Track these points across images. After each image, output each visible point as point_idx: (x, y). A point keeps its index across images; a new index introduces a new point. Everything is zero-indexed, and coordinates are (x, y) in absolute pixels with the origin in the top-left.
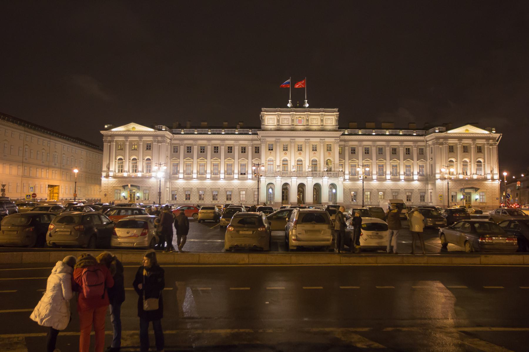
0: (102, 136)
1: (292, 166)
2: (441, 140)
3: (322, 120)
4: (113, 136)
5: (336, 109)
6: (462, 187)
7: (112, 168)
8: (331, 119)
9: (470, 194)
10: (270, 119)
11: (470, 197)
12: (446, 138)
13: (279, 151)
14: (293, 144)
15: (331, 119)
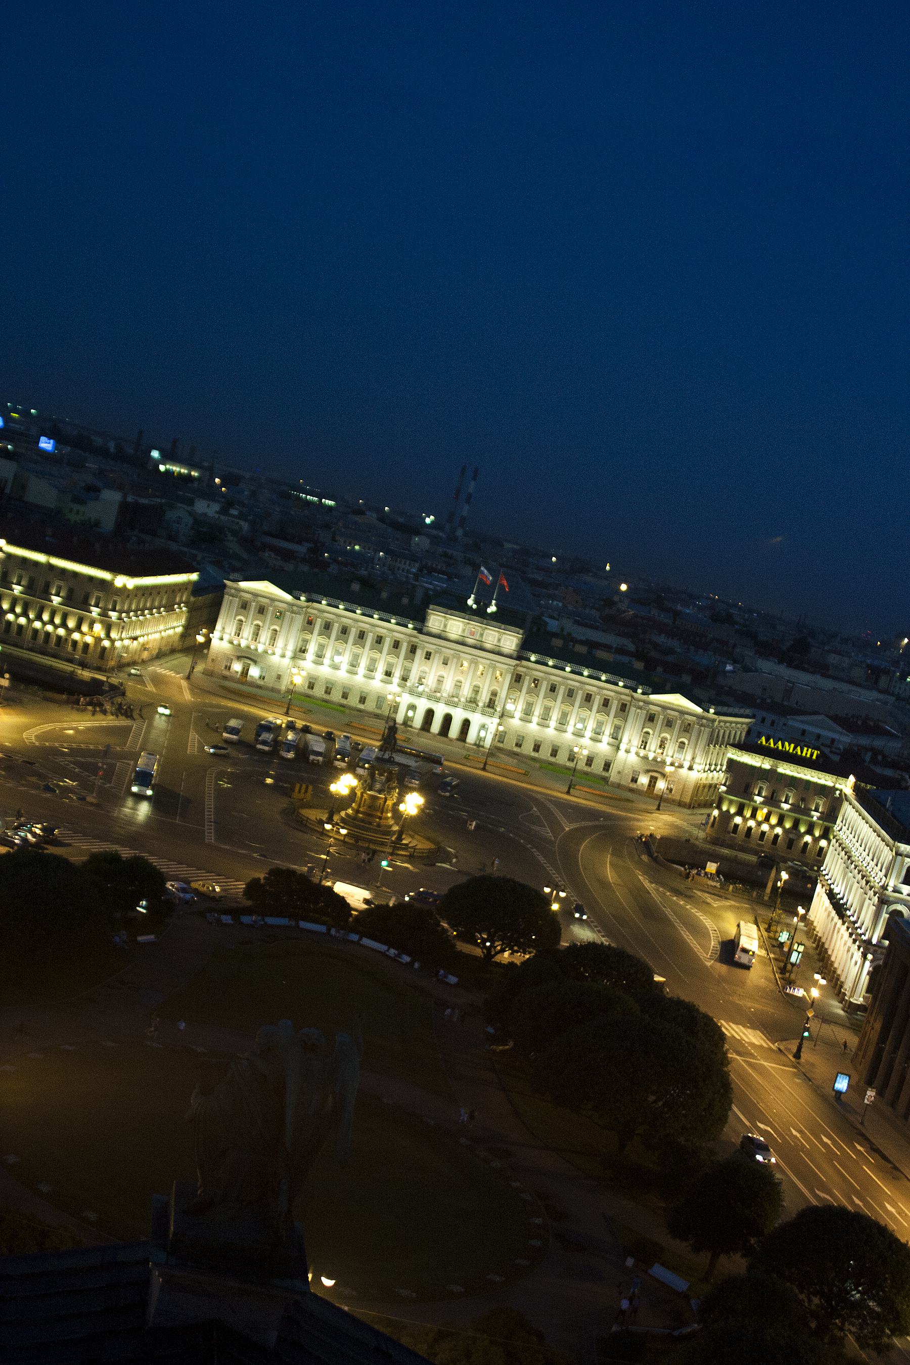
0: (225, 586)
1: (448, 687)
2: (641, 704)
3: (499, 640)
4: (239, 590)
5: (521, 631)
6: (648, 768)
7: (227, 630)
8: (510, 641)
9: (656, 778)
10: (436, 620)
11: (655, 783)
12: (648, 703)
13: (436, 660)
14: (455, 660)
15: (510, 641)
